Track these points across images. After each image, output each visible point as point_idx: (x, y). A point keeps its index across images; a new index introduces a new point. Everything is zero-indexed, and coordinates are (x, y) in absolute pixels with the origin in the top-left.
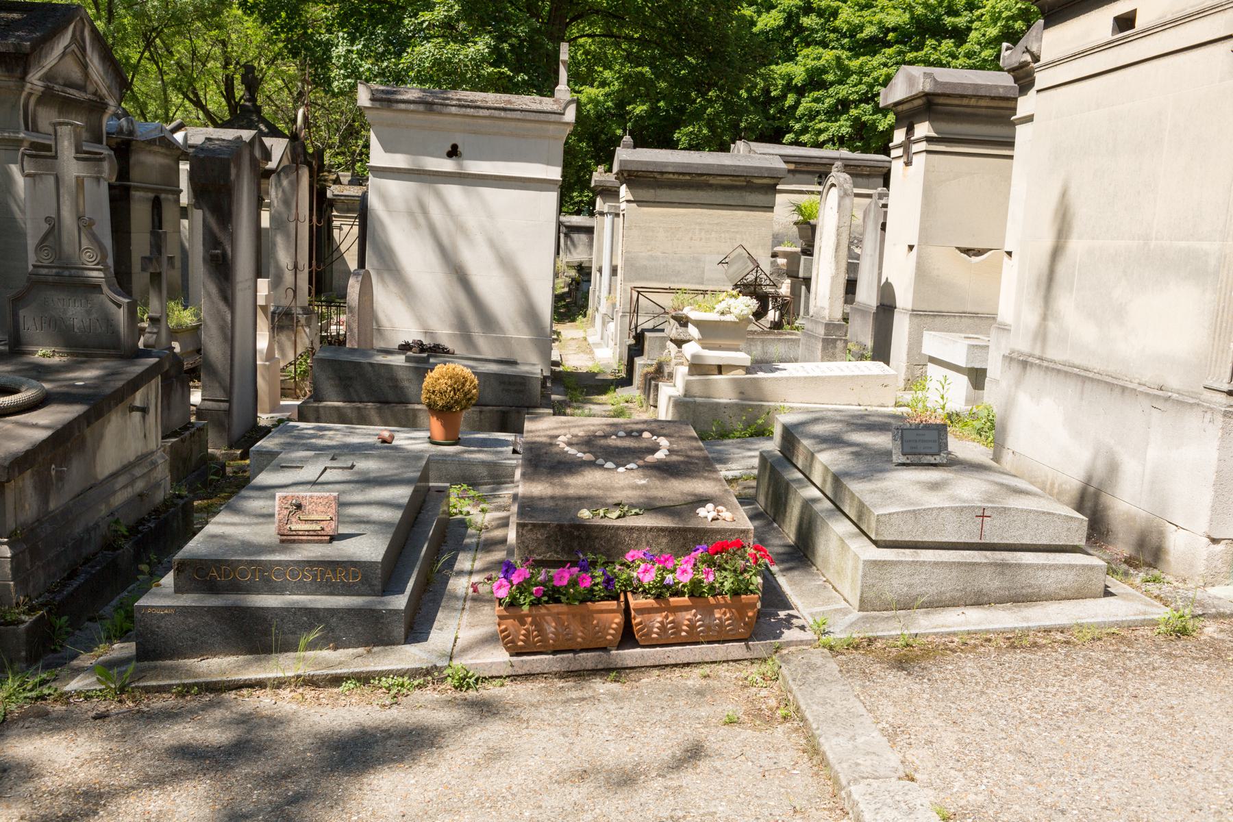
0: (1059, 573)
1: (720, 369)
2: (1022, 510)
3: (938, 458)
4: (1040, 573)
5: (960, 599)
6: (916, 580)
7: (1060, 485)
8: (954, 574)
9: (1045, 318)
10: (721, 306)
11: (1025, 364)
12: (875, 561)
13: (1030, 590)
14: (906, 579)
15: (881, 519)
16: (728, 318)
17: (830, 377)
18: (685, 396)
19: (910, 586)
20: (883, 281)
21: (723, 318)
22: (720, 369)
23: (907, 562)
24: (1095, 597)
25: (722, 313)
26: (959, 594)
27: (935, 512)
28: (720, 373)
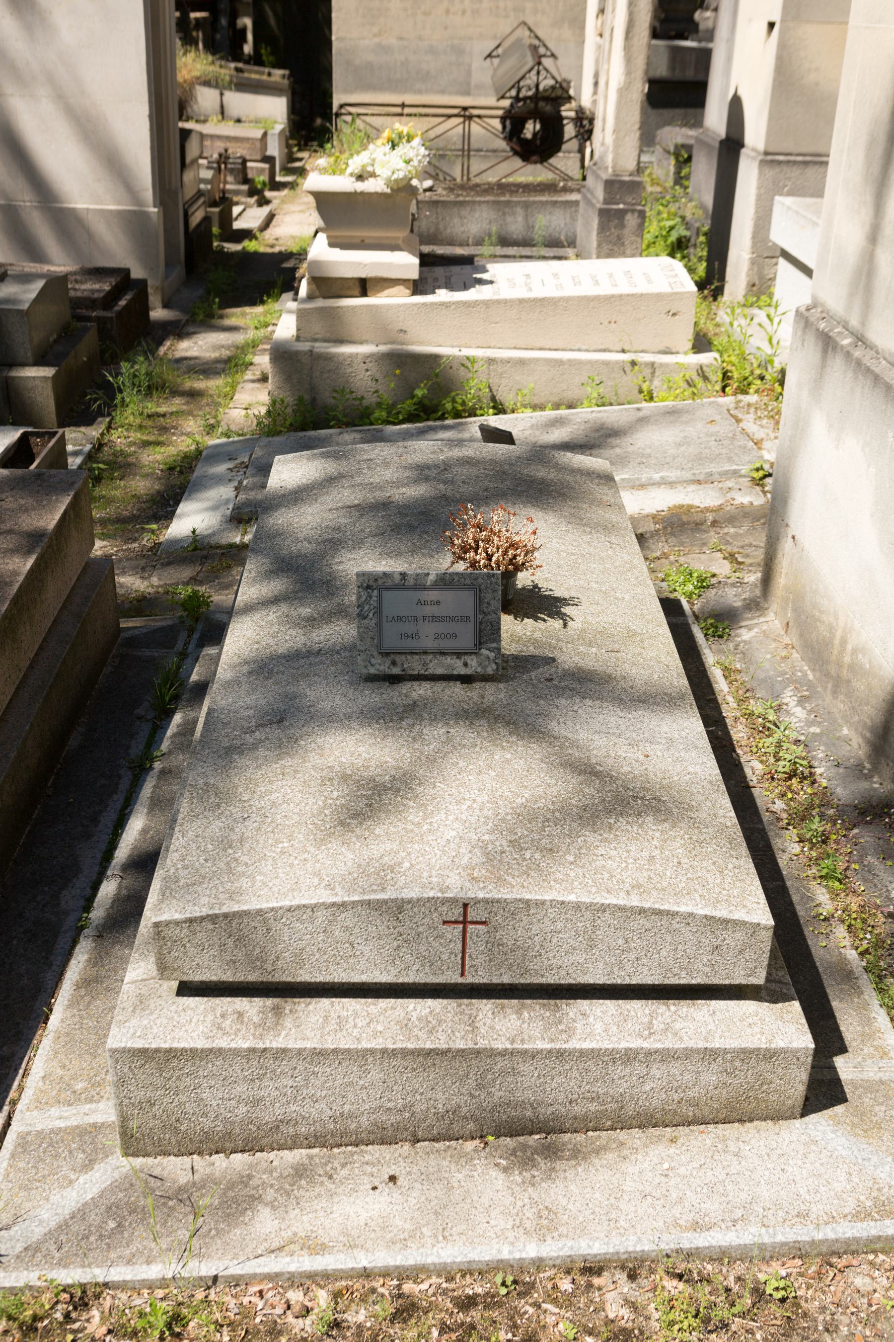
0: (675, 1068)
1: (364, 286)
2: (578, 907)
3: (473, 662)
4: (619, 1070)
5: (398, 1128)
6: (268, 1089)
7: (855, 651)
8: (219, 1242)
9: (874, 236)
10: (356, 163)
11: (827, 343)
12: (143, 1052)
13: (593, 1107)
14: (239, 1089)
15: (167, 932)
16: (371, 186)
17: (568, 299)
18: (298, 338)
19: (256, 1102)
20: (235, 199)
21: (360, 187)
22: (364, 286)
23: (236, 1052)
24: (777, 1116)
25: (360, 178)
26: (393, 1118)
27: (321, 915)
28: (364, 293)
